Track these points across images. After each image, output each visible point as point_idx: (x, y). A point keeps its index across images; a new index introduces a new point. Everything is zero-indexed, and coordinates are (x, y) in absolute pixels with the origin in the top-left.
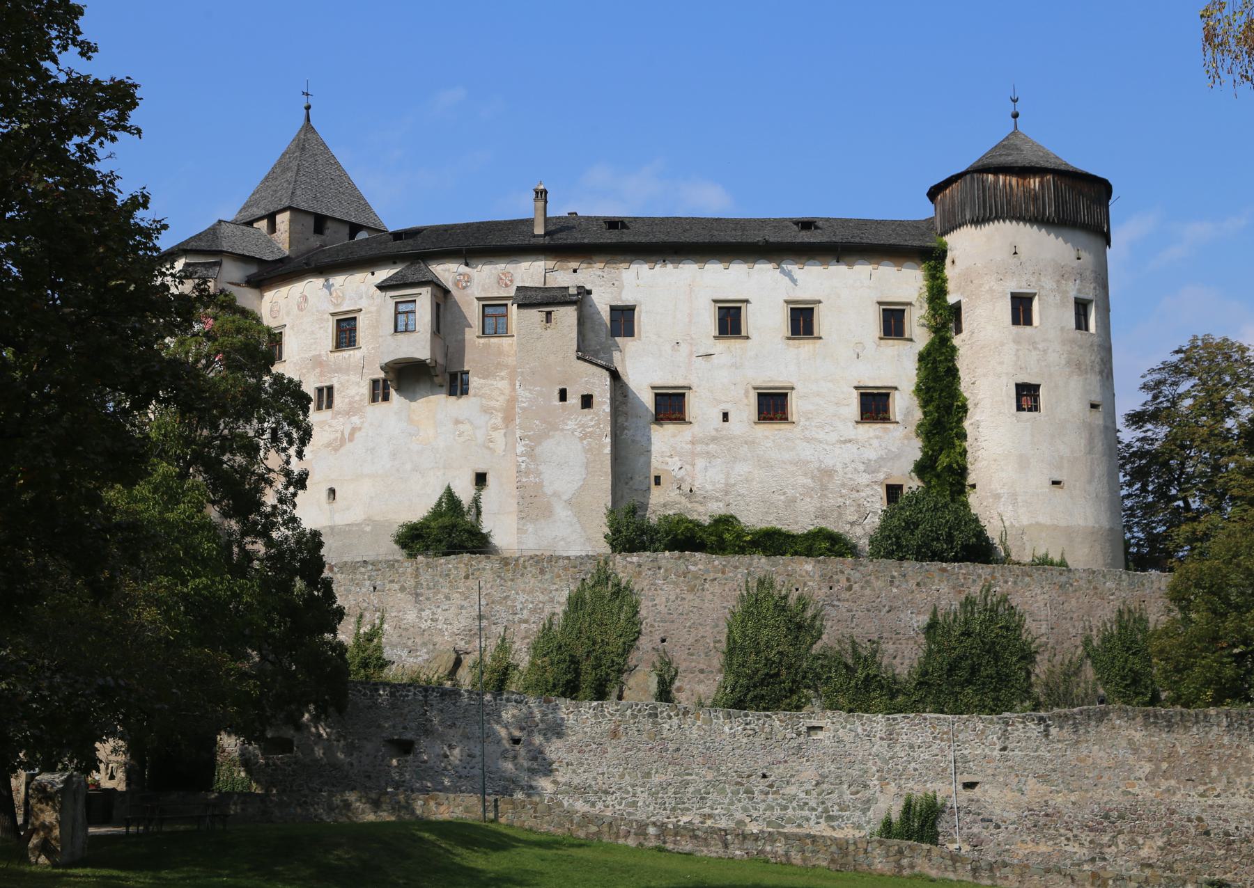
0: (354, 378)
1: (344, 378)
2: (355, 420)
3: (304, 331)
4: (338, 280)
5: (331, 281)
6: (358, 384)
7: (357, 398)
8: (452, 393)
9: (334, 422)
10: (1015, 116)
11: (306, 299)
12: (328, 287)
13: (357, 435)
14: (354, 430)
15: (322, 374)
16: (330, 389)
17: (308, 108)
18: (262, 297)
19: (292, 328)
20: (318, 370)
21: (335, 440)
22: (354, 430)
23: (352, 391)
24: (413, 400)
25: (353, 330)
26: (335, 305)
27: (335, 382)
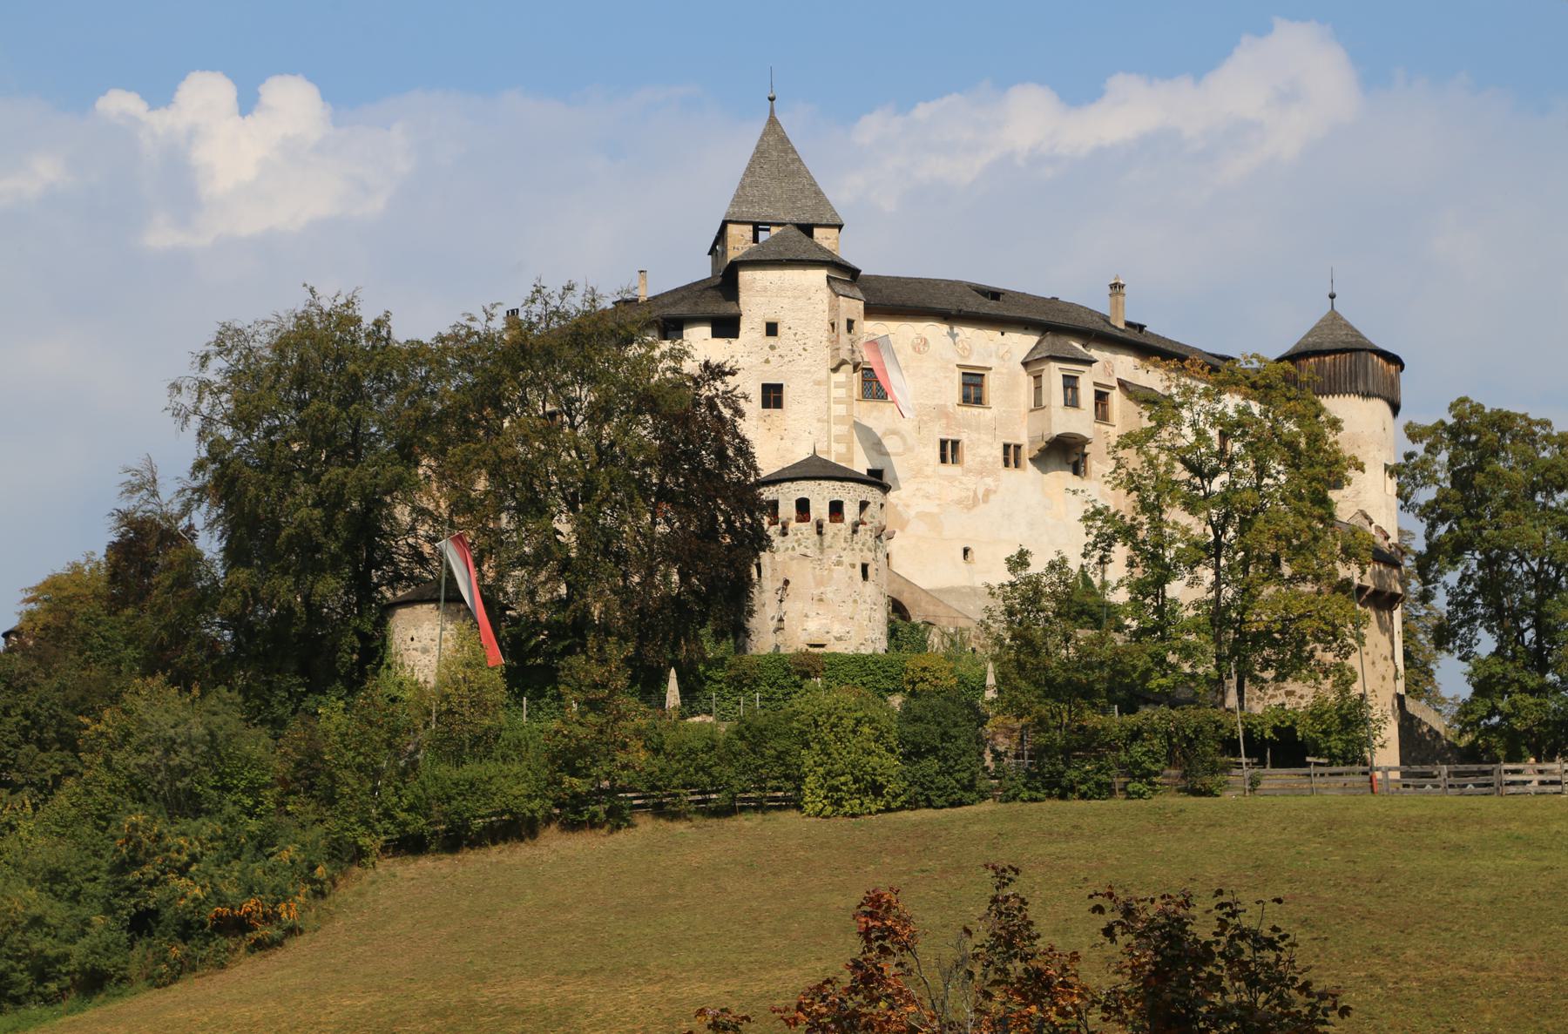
0: (986, 438)
1: (974, 436)
2: (989, 481)
4: (966, 332)
5: (956, 330)
6: (990, 445)
7: (990, 459)
8: (1076, 472)
9: (965, 479)
10: (1332, 297)
11: (926, 342)
12: (953, 336)
13: (992, 497)
14: (988, 493)
15: (948, 426)
16: (955, 443)
20: (944, 421)
21: (967, 498)
22: (988, 493)
23: (984, 451)
24: (1044, 472)
25: (980, 386)
26: (962, 357)
27: (964, 438)
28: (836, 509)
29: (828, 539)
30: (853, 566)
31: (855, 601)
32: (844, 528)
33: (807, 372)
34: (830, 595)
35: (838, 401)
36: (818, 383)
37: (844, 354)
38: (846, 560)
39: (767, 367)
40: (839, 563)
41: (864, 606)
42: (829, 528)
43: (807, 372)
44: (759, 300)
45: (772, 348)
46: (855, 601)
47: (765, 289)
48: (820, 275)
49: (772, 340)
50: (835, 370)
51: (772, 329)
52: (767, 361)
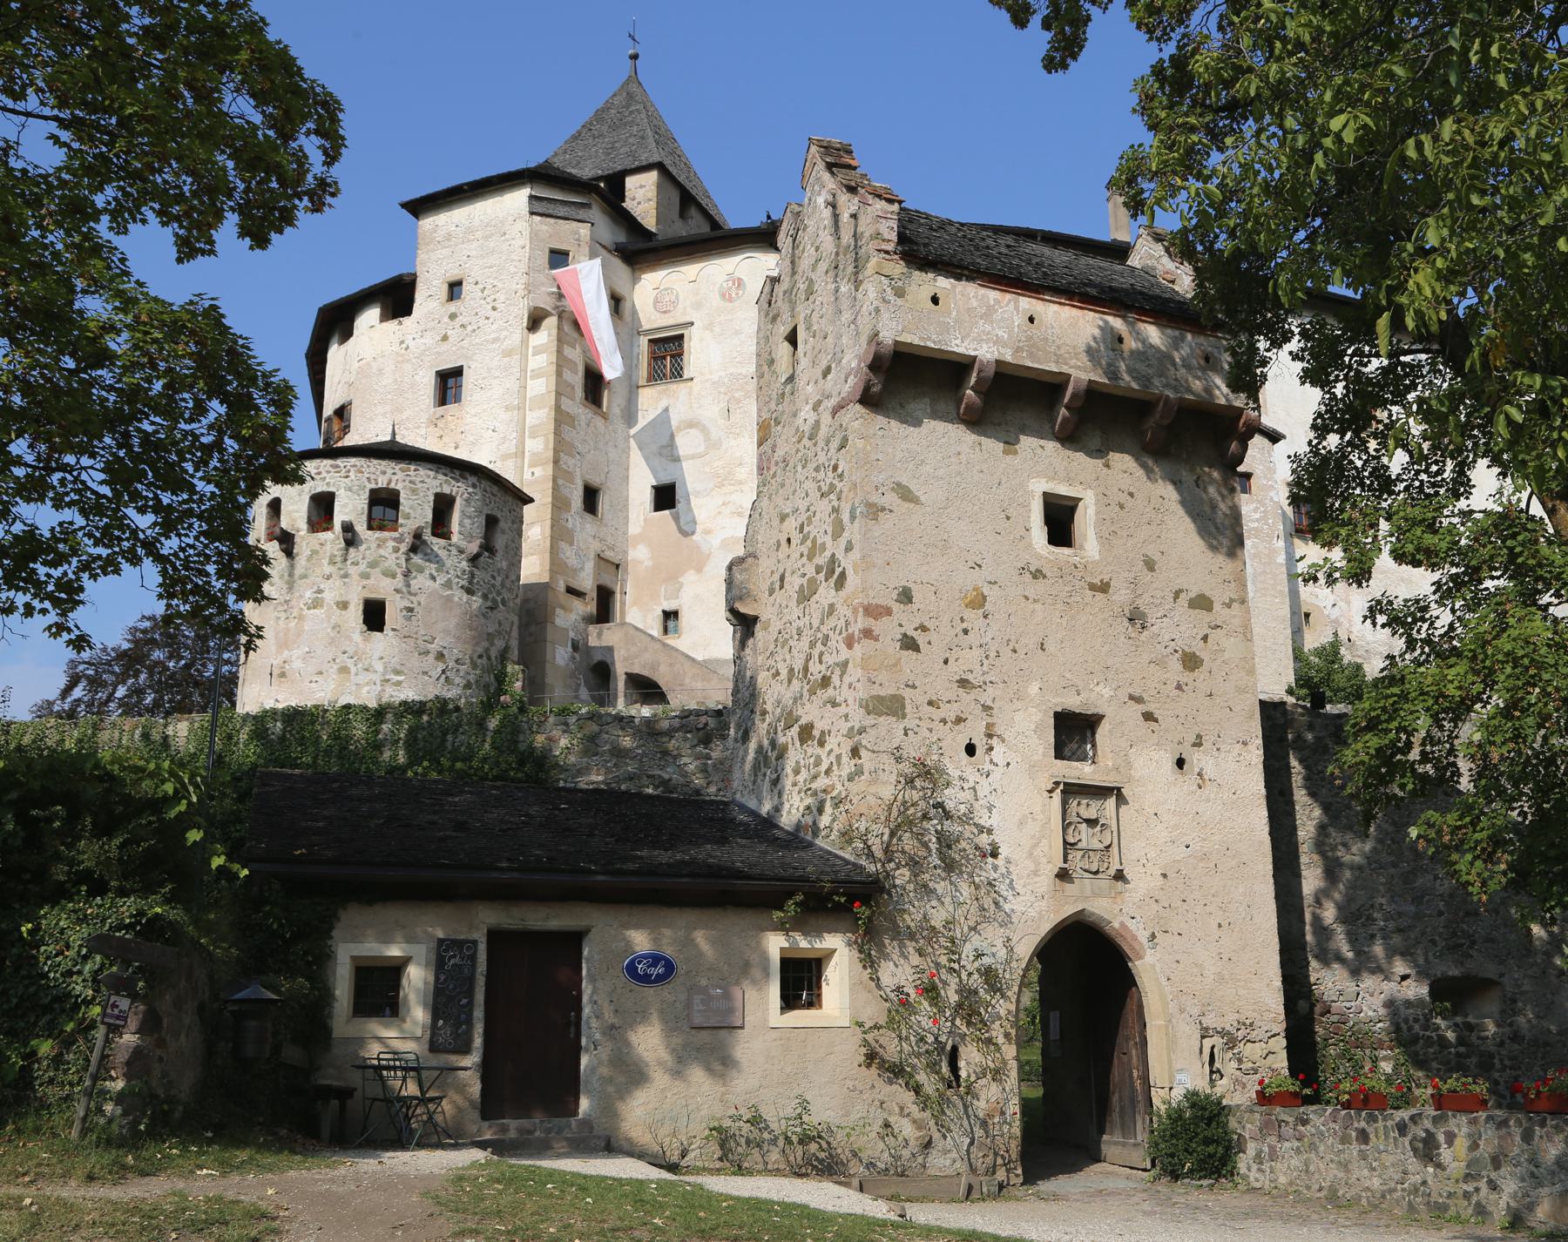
3: (737, 333)
17: (635, 57)
18: (635, 281)
19: (709, 327)
28: (323, 506)
29: (301, 561)
30: (344, 605)
31: (344, 670)
32: (331, 539)
33: (495, 340)
34: (297, 664)
35: (537, 375)
36: (508, 353)
37: (547, 303)
38: (329, 596)
39: (445, 346)
40: (316, 604)
41: (363, 678)
42: (305, 542)
43: (495, 340)
44: (442, 253)
45: (453, 316)
46: (344, 670)
47: (449, 236)
48: (518, 199)
49: (453, 307)
50: (534, 323)
51: (455, 289)
52: (445, 338)
